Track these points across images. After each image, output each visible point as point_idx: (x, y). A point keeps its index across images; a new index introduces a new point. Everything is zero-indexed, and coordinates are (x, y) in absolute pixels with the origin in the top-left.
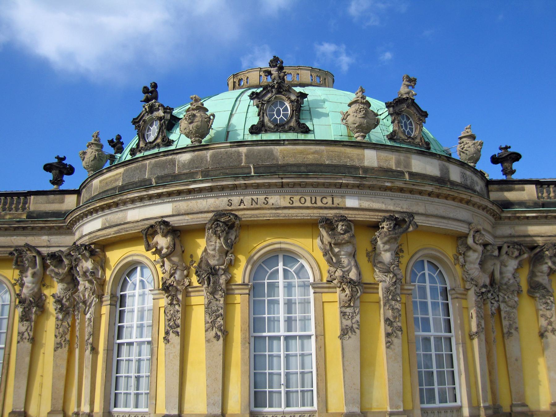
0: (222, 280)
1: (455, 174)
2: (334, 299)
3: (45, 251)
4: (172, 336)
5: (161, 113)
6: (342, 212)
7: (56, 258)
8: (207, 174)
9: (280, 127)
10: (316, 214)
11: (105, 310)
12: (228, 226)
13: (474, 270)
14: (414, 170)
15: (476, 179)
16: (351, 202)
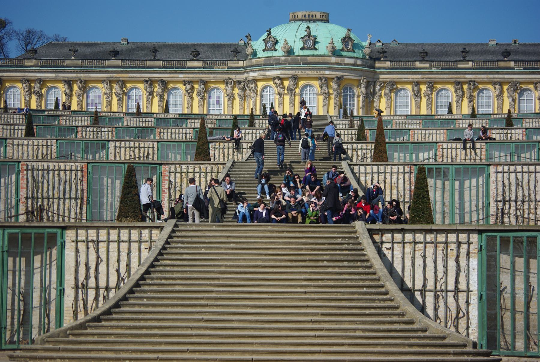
0: (293, 92)
1: (359, 62)
2: (321, 98)
3: (235, 80)
4: (280, 106)
5: (273, 39)
6: (325, 76)
7: (239, 82)
8: (289, 64)
9: (309, 49)
10: (318, 76)
11: (258, 99)
12: (295, 79)
13: (363, 90)
14: (346, 62)
15: (367, 61)
16: (327, 72)
